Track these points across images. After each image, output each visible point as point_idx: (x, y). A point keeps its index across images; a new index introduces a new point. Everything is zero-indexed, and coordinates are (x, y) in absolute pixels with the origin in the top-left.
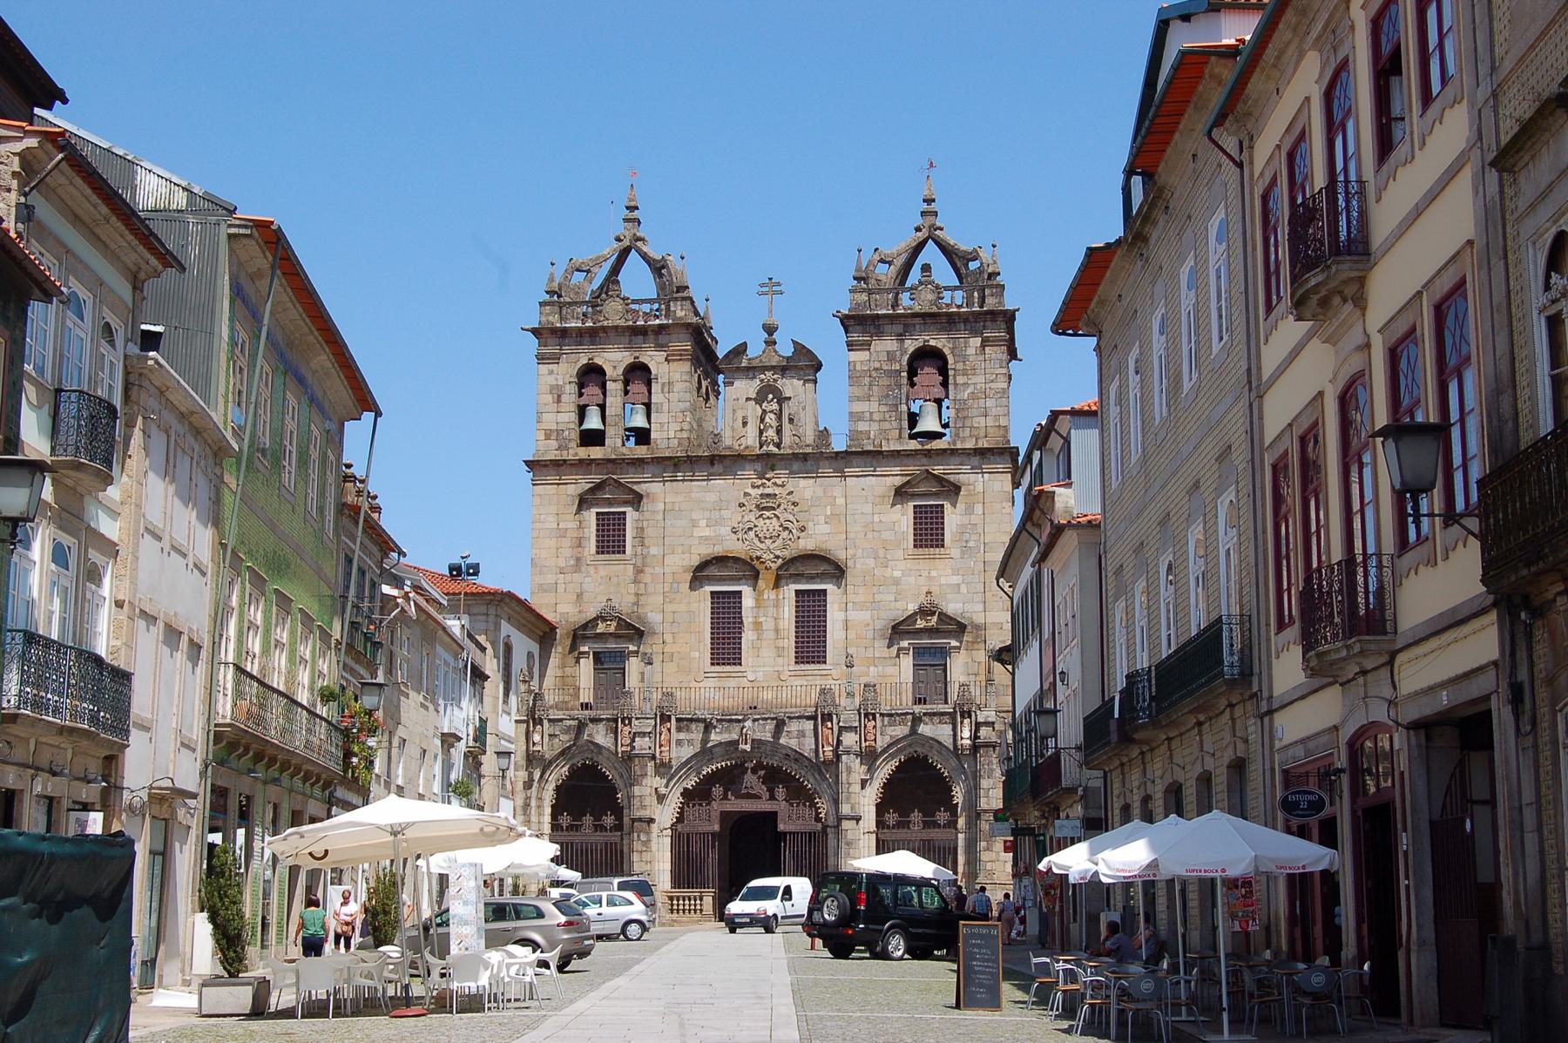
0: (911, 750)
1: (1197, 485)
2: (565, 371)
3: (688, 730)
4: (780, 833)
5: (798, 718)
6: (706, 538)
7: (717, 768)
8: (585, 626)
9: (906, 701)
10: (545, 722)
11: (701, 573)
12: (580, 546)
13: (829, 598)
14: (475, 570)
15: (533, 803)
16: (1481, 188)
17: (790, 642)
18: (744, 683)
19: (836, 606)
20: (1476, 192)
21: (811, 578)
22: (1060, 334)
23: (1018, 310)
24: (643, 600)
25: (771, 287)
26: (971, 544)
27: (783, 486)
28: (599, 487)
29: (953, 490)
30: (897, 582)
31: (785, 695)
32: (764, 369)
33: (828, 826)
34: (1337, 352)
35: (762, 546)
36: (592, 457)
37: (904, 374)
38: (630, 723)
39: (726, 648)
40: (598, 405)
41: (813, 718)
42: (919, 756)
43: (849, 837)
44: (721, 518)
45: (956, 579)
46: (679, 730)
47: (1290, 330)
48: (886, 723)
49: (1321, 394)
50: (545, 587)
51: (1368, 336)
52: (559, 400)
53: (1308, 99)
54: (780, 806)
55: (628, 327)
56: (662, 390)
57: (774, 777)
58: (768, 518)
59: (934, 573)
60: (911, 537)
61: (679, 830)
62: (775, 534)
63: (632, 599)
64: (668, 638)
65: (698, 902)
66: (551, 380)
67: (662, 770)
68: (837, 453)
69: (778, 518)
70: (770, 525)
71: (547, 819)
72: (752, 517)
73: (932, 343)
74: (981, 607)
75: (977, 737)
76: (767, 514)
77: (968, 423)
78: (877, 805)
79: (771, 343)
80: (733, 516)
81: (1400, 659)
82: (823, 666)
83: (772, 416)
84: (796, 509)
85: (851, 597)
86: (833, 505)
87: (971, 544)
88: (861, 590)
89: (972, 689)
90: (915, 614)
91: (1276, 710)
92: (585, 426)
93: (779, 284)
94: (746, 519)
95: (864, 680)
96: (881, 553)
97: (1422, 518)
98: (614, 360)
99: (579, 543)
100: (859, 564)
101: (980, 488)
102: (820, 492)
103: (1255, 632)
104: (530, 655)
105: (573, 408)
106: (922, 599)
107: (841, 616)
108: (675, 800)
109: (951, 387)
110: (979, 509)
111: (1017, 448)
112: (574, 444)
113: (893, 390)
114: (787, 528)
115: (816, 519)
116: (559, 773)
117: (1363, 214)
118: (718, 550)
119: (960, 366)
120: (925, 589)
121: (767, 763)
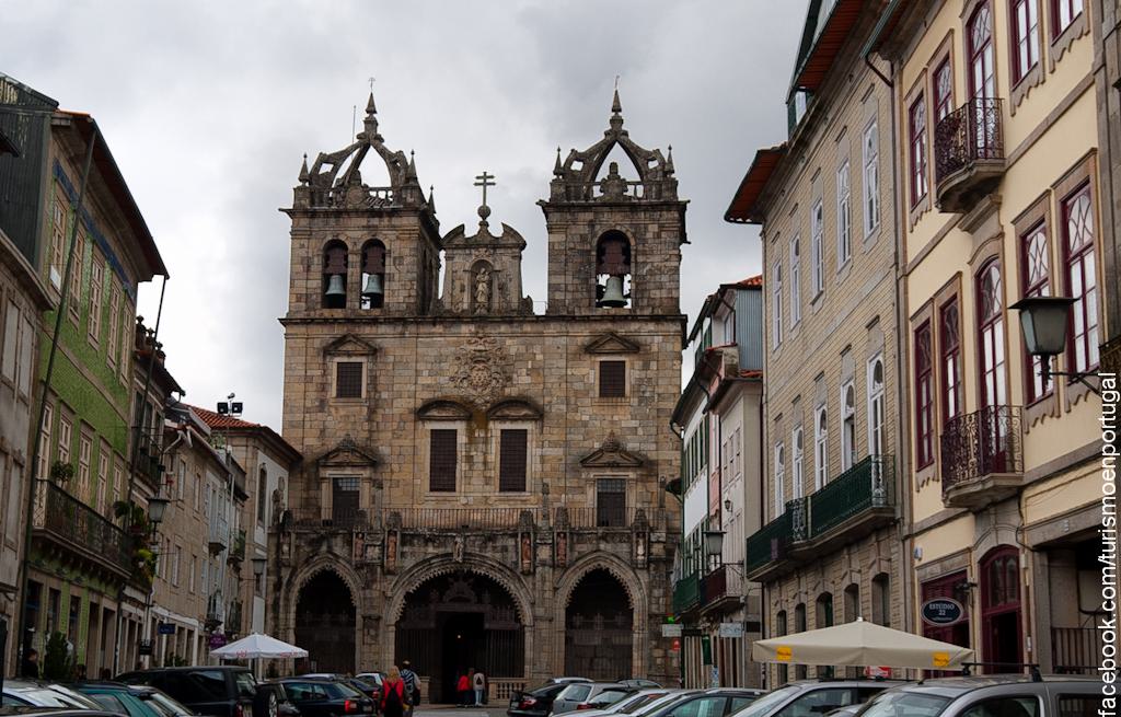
0: (595, 564)
1: (848, 347)
2: (315, 247)
3: (412, 544)
6: (429, 386)
8: (327, 456)
9: (589, 521)
10: (293, 536)
11: (421, 413)
12: (323, 390)
13: (529, 437)
14: (238, 407)
15: (281, 603)
16: (1104, 105)
17: (495, 473)
18: (458, 505)
19: (534, 443)
20: (1099, 109)
22: (731, 222)
24: (375, 435)
25: (485, 181)
26: (647, 394)
28: (342, 341)
29: (633, 347)
30: (585, 424)
31: (491, 516)
33: (525, 626)
34: (973, 239)
35: (474, 392)
36: (336, 317)
37: (594, 253)
38: (363, 538)
39: (443, 477)
40: (341, 274)
41: (515, 536)
43: (543, 635)
44: (441, 370)
45: (634, 423)
46: (403, 544)
47: (936, 220)
48: (575, 540)
49: (959, 274)
50: (294, 423)
51: (1002, 227)
53: (952, 31)
54: (486, 608)
55: (367, 211)
56: (394, 264)
57: (484, 585)
58: (479, 370)
59: (616, 418)
60: (597, 388)
63: (366, 434)
64: (395, 467)
66: (303, 253)
67: (389, 577)
68: (538, 317)
70: (479, 375)
71: (292, 616)
72: (467, 367)
73: (618, 228)
74: (653, 446)
75: (650, 554)
76: (481, 366)
77: (646, 295)
78: (567, 609)
79: (484, 225)
80: (450, 368)
81: (1027, 493)
82: (523, 494)
83: (485, 285)
84: (503, 363)
85: (547, 437)
86: (534, 360)
87: (647, 394)
88: (556, 431)
89: (647, 514)
90: (601, 450)
91: (917, 534)
92: (329, 292)
93: (492, 177)
95: (556, 505)
96: (573, 400)
97: (1066, 371)
98: (354, 234)
99: (323, 388)
100: (557, 408)
102: (522, 349)
103: (898, 469)
104: (281, 480)
105: (319, 276)
107: (539, 451)
108: (399, 601)
109: (633, 265)
110: (654, 365)
111: (686, 316)
112: (319, 306)
113: (584, 267)
116: (304, 575)
117: (999, 126)
118: (438, 394)
119: (640, 247)
120: (609, 431)
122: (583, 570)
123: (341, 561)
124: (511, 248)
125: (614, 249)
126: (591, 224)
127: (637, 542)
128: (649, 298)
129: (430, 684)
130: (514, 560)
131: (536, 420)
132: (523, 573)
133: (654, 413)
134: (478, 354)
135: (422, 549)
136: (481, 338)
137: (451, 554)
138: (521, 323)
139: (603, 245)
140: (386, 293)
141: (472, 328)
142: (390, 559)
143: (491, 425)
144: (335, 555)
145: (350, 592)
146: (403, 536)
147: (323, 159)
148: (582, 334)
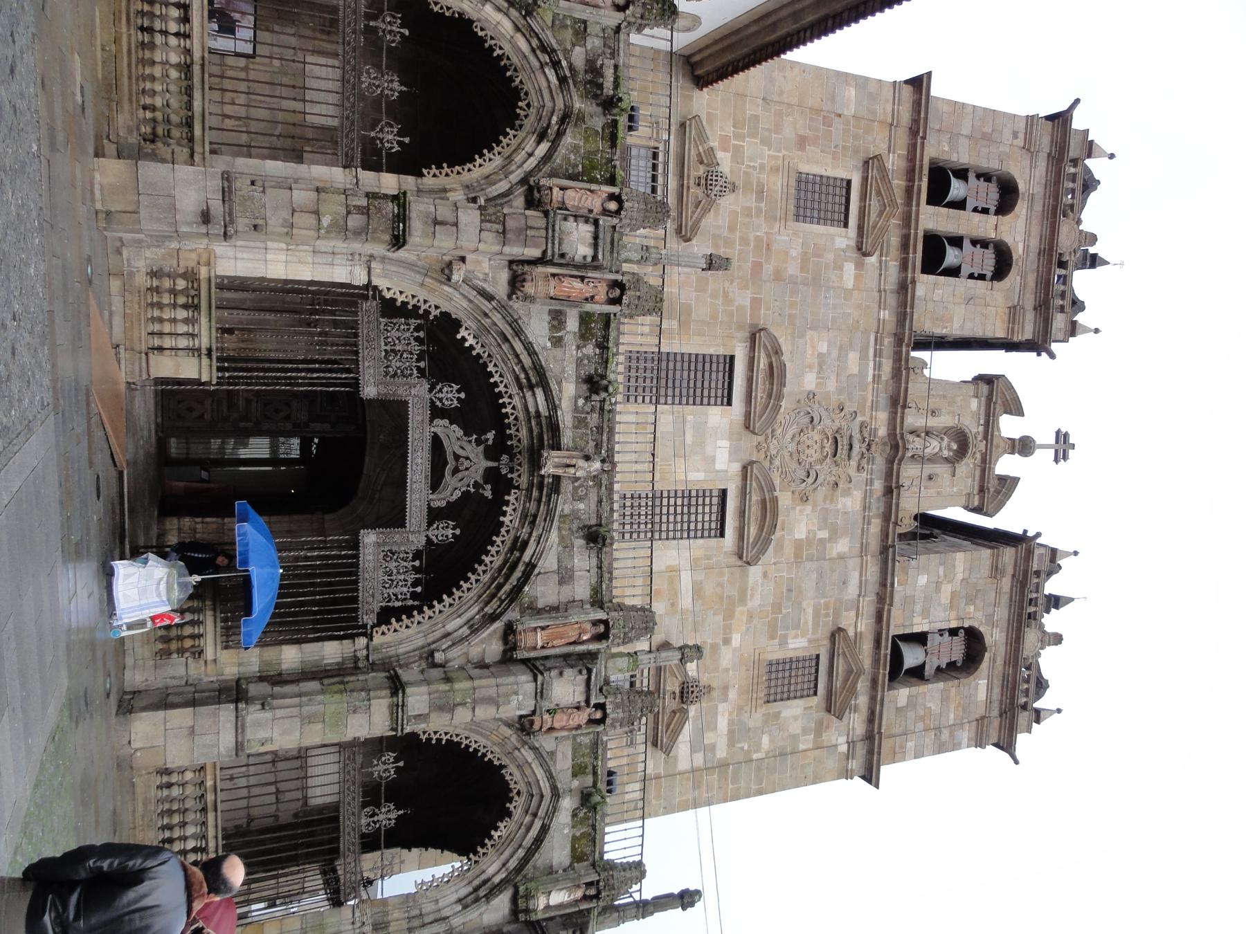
4: (356, 535)
5: (600, 568)
7: (500, 395)
10: (614, 18)
13: (714, 542)
19: (699, 553)
21: (742, 513)
23: (1016, 762)
27: (860, 468)
29: (834, 706)
33: (370, 638)
41: (598, 600)
42: (511, 800)
58: (823, 447)
59: (733, 694)
61: (366, 305)
62: (803, 457)
65: (183, 342)
66: (1007, 135)
67: (504, 276)
69: (821, 461)
72: (827, 422)
73: (987, 655)
83: (937, 450)
93: (1065, 458)
94: (824, 414)
106: (704, 680)
114: (808, 476)
121: (507, 503)
122: (505, 761)
123: (544, 147)
124: (982, 490)
125: (956, 650)
127: (578, 886)
129: (198, 382)
132: (509, 630)
134: (846, 441)
135: (571, 370)
137: (557, 446)
138: (886, 517)
139: (962, 631)
140: (942, 278)
141: (882, 432)
142: (553, 283)
144: (560, 134)
145: (462, 163)
146: (607, 320)
147: (1090, 184)
148: (860, 625)
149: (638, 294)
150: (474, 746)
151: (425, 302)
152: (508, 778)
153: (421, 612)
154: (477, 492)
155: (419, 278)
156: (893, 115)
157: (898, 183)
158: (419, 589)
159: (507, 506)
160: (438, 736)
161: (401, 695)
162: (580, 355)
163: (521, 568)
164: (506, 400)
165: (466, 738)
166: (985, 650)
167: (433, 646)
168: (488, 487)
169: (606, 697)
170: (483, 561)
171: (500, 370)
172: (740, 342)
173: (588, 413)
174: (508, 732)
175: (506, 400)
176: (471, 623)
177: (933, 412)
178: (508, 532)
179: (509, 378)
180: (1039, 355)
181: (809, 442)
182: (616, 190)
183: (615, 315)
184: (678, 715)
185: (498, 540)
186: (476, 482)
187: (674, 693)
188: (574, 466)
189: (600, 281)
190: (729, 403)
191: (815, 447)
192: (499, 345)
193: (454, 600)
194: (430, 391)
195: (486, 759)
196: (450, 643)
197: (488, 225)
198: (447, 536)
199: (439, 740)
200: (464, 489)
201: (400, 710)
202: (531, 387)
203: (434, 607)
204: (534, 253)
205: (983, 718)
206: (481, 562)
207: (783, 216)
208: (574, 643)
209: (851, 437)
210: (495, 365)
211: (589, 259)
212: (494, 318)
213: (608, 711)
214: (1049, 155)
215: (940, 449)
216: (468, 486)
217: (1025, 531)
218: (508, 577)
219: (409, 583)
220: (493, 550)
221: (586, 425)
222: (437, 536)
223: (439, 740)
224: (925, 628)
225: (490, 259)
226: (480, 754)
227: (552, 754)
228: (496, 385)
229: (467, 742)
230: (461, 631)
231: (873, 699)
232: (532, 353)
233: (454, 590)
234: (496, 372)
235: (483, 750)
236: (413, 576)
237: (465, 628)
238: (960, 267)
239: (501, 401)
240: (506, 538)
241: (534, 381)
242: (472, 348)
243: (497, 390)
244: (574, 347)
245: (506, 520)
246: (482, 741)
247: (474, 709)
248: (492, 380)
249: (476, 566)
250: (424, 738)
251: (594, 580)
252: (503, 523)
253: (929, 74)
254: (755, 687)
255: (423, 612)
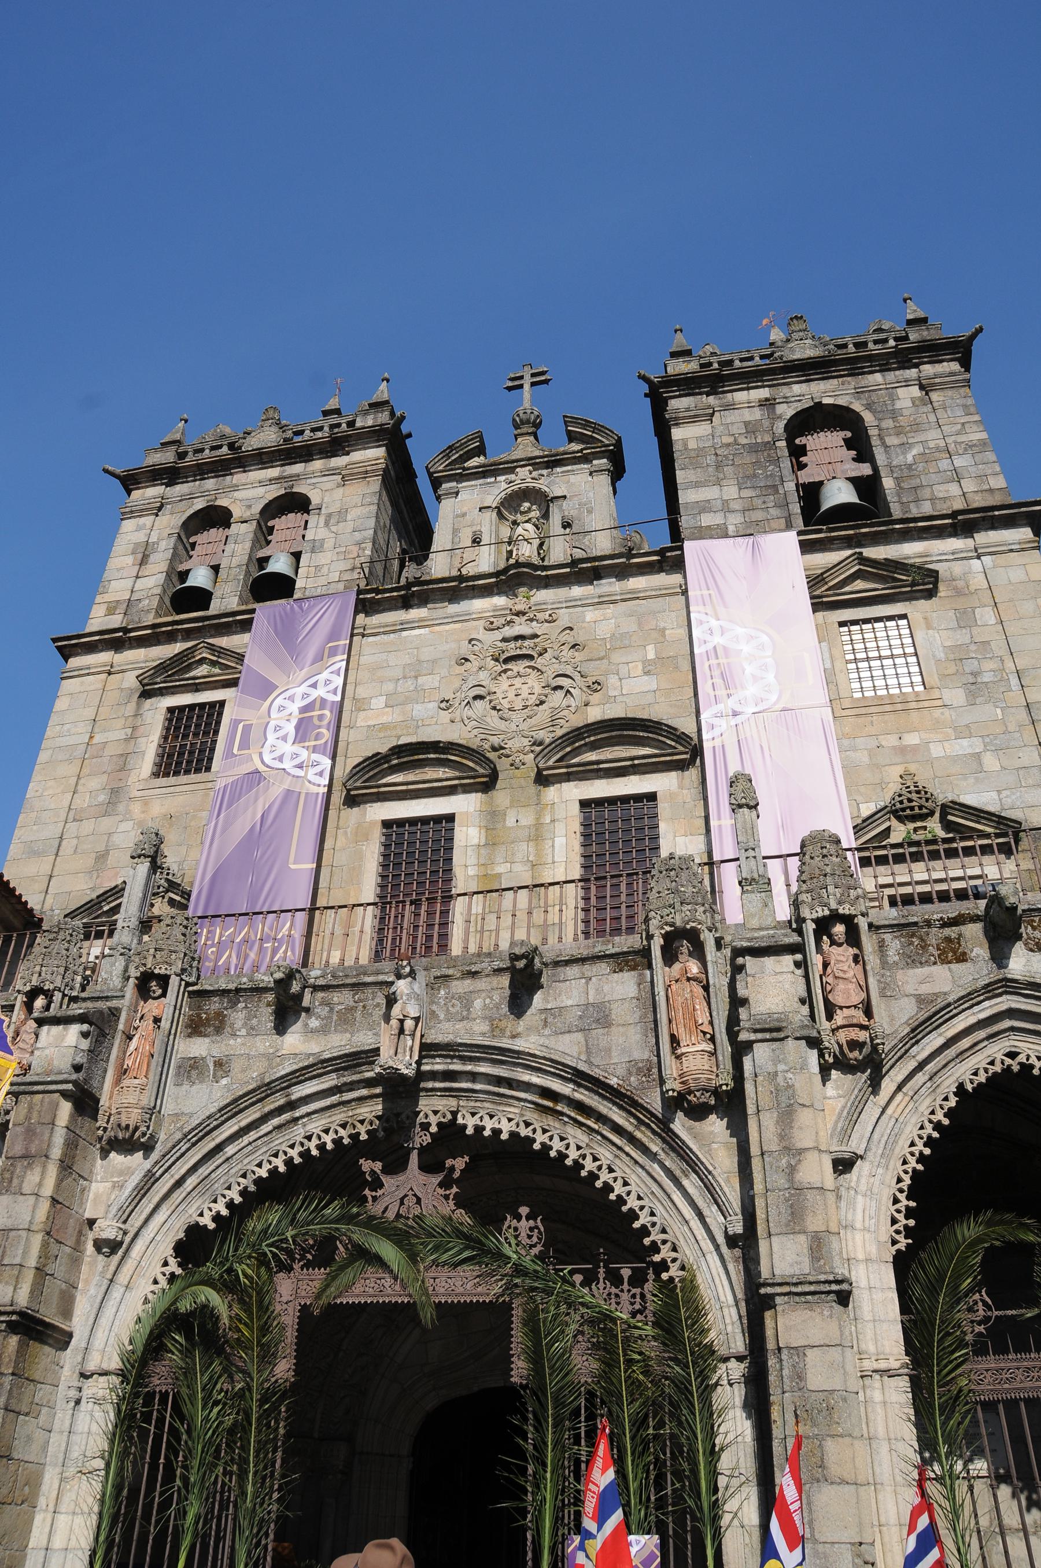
0: (997, 1050)
6: (384, 727)
7: (305, 1154)
12: (122, 769)
13: (663, 808)
23: (980, 330)
26: (987, 677)
28: (180, 664)
32: (509, 468)
35: (502, 725)
45: (965, 746)
48: (892, 956)
52: (144, 561)
59: (912, 739)
66: (141, 537)
73: (826, 401)
77: (926, 493)
78: (902, 1264)
83: (529, 526)
84: (579, 656)
94: (472, 682)
101: (978, 581)
102: (630, 625)
105: (164, 566)
110: (986, 616)
112: (151, 616)
114: (561, 687)
115: (624, 670)
121: (479, 1129)
122: (948, 1084)
124: (586, 459)
126: (767, 404)
128: (933, 500)
130: (643, 1054)
131: (681, 766)
133: (1023, 714)
134: (512, 645)
136: (519, 614)
138: (622, 572)
139: (797, 441)
140: (300, 570)
142: (126, 1082)
143: (552, 793)
149: (152, 951)
150: (920, 1145)
151: (156, 1282)
152: (982, 1078)
153: (663, 1266)
154: (457, 1182)
155: (117, 1293)
156: (99, 673)
157: (178, 647)
158: (626, 1273)
159: (483, 1128)
160: (900, 1217)
161: (769, 1290)
162: (243, 1032)
163: (582, 1096)
164: (312, 1145)
165: (905, 1162)
166: (819, 404)
167: (721, 1239)
168: (449, 1162)
169: (804, 920)
170: (576, 1162)
171: (265, 1157)
172: (365, 814)
173: (332, 1009)
174: (888, 1085)
175: (312, 1145)
176: (678, 1173)
177: (474, 541)
178: (527, 1124)
179: (280, 1142)
180: (409, 435)
181: (511, 695)
182: (21, 999)
183: (188, 984)
184: (950, 818)
185: (540, 1138)
186: (441, 1185)
187: (915, 830)
188: (402, 1021)
189: (136, 1011)
190: (450, 818)
191: (518, 686)
192: (228, 1159)
193: (642, 1208)
194: (289, 1269)
195: (946, 1122)
196: (714, 1208)
197: (15, 1182)
198: (531, 1229)
199: (909, 1213)
200: (451, 1203)
201: (799, 1289)
202: (291, 1105)
203: (654, 1243)
204: (66, 1108)
205: (922, 387)
206: (578, 1166)
207: (202, 786)
208: (706, 988)
209: (505, 640)
210: (260, 1165)
211: (85, 1027)
212: (183, 1171)
213: (827, 912)
214: (167, 485)
215: (527, 522)
216: (446, 1197)
217: (646, 395)
218: (601, 1118)
219: (614, 1290)
220: (557, 1145)
221: (351, 1009)
222: (531, 1246)
223: (909, 1213)
224: (791, 486)
225: (97, 1181)
226: (936, 1135)
227: (921, 1000)
228: (289, 1162)
229: (913, 1163)
230: (691, 1190)
231: (907, 535)
232: (232, 1108)
233: (624, 1209)
234: (270, 1162)
235: (929, 1129)
236: (601, 1285)
237: (685, 1183)
238: (292, 554)
239: (315, 1152)
240: (537, 1125)
241: (282, 1102)
242: (230, 1205)
243: (297, 1160)
244: (232, 1042)
245: (506, 1128)
246: (911, 1131)
247: (801, 1151)
248: (282, 1169)
249: (584, 1173)
250: (903, 1243)
251: (603, 967)
252: (513, 1135)
253: (54, 640)
254: (899, 707)
255: (664, 1261)
